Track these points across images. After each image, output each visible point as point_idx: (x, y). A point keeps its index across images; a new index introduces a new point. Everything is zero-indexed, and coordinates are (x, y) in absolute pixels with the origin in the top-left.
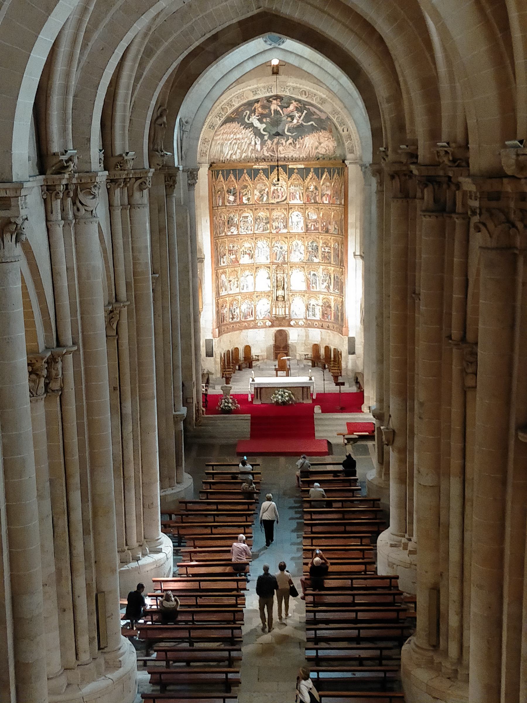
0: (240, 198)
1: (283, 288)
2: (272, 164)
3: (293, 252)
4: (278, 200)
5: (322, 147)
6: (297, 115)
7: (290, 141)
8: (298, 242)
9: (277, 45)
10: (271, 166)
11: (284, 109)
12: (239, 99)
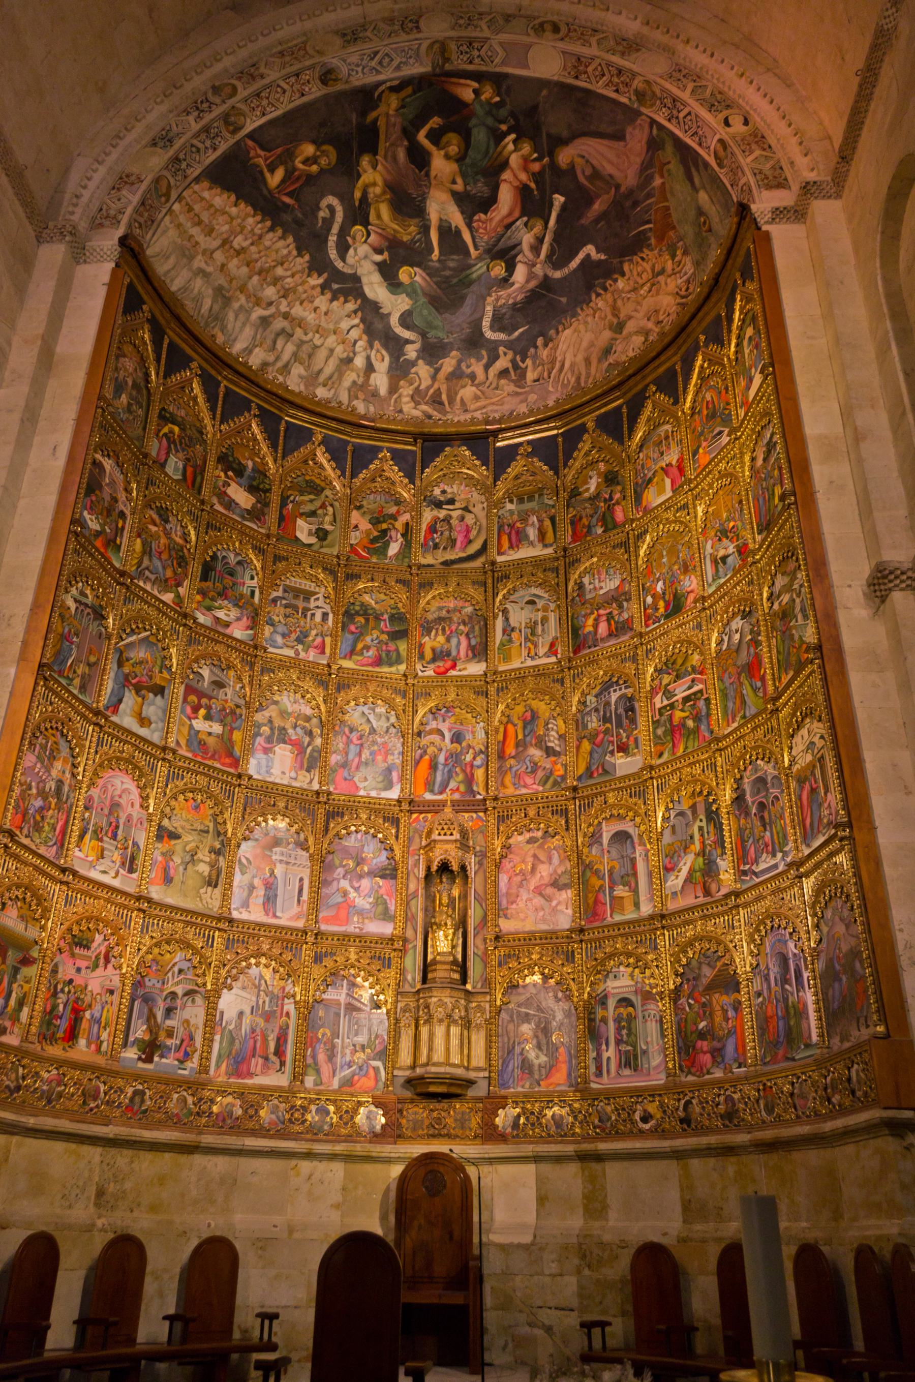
0: (281, 518)
1: (462, 924)
3: (510, 750)
7: (503, 363)
12: (287, 59)
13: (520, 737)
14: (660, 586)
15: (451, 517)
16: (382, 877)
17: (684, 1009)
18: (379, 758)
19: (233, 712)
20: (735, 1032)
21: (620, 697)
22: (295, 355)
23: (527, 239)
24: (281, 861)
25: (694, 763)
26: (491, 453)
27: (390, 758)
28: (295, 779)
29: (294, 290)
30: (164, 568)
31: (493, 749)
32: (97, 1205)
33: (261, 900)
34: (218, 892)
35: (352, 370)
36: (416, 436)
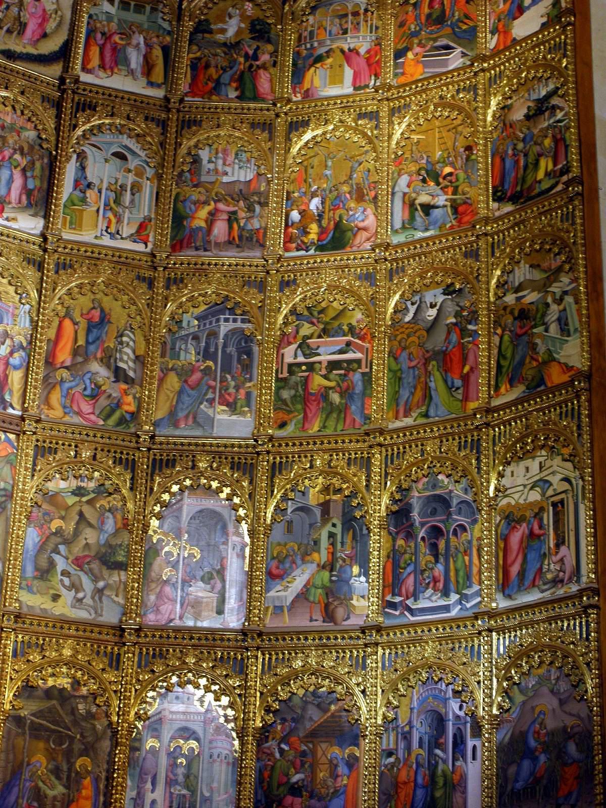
3: (64, 356)
13: (81, 342)
17: (272, 754)
20: (345, 792)
21: (233, 332)
25: (337, 451)
31: (43, 347)
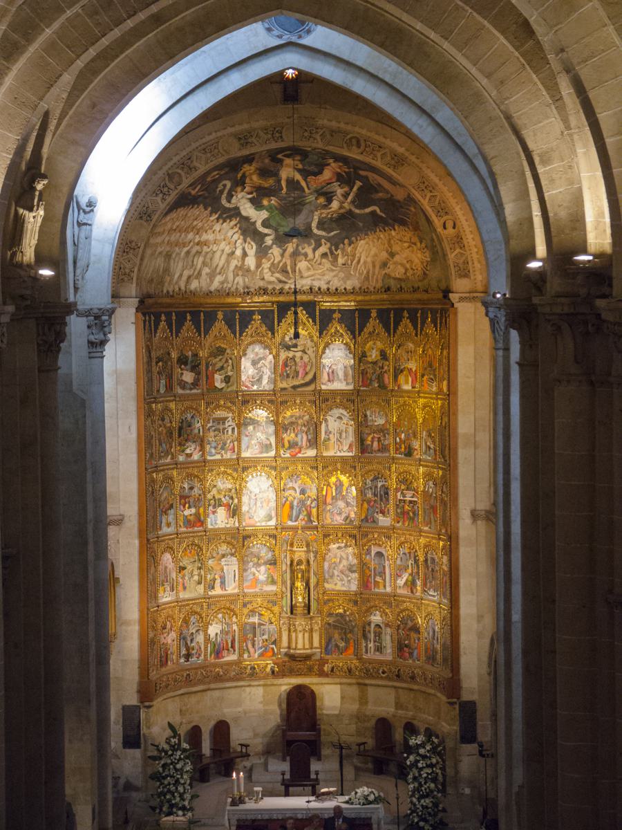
2: (281, 299)
3: (329, 500)
4: (296, 383)
5: (395, 263)
6: (340, 191)
8: (344, 479)
9: (294, 39)
10: (277, 302)
11: (310, 178)
12: (209, 155)
13: (334, 494)
14: (403, 435)
15: (294, 356)
16: (270, 564)
18: (265, 504)
19: (198, 499)
21: (383, 486)
22: (204, 264)
23: (340, 191)
24: (225, 565)
26: (317, 314)
27: (271, 503)
28: (227, 523)
29: (202, 228)
30: (166, 445)
32: (181, 715)
33: (219, 584)
34: (202, 585)
35: (235, 259)
36: (273, 303)
